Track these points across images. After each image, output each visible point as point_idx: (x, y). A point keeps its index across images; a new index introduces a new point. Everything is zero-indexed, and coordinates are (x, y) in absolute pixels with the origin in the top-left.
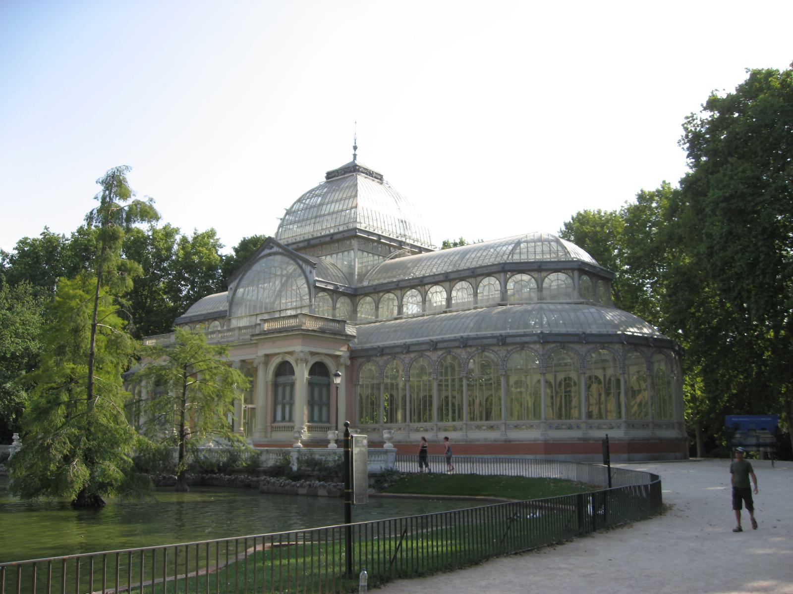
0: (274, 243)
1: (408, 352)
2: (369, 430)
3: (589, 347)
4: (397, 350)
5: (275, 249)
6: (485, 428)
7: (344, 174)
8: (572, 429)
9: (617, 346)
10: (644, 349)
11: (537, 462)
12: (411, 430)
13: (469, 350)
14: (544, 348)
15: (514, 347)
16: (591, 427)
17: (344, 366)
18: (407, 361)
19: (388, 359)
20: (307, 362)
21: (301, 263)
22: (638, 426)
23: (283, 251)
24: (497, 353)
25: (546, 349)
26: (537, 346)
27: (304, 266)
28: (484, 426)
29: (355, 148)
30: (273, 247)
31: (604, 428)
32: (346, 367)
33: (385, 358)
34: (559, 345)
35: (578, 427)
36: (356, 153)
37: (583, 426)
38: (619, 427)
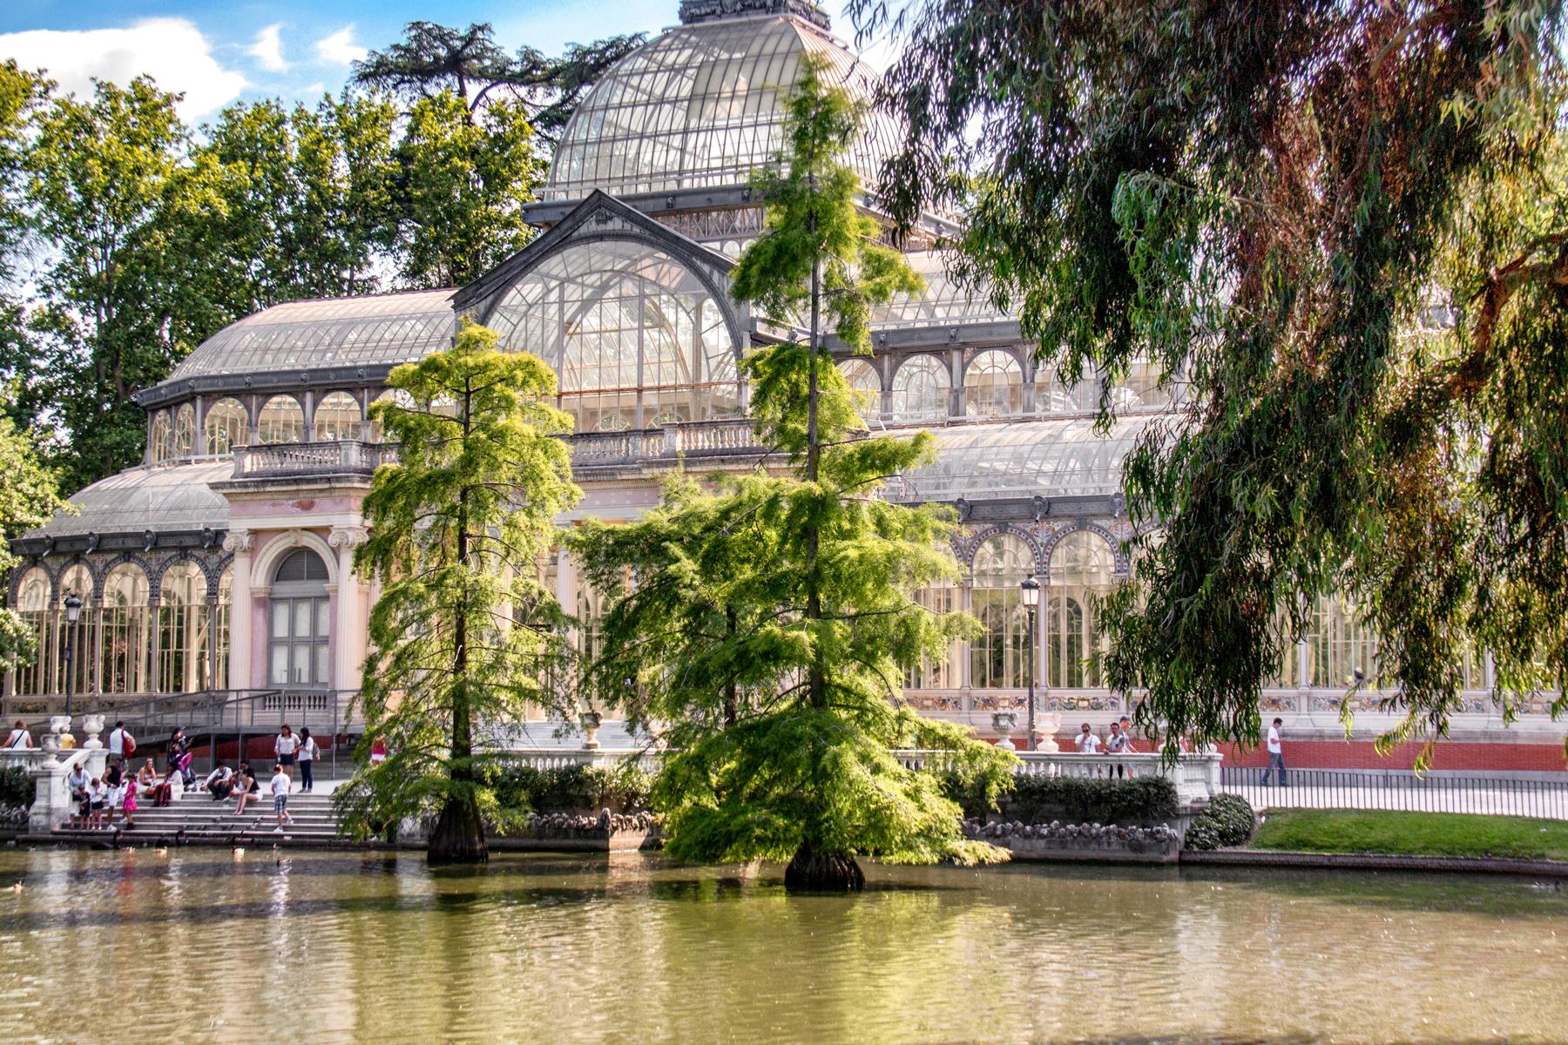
0: (612, 210)
1: (1047, 515)
2: (929, 703)
4: (1014, 511)
5: (616, 224)
7: (739, 13)
11: (1387, 784)
12: (1053, 705)
18: (1041, 538)
19: (985, 531)
21: (706, 268)
23: (647, 234)
27: (716, 276)
30: (611, 218)
33: (977, 528)
35: (1479, 708)
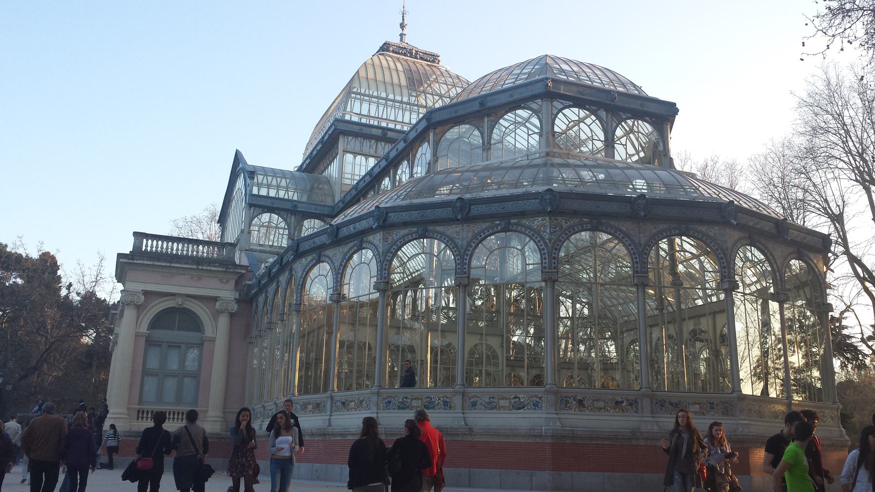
3: (477, 227)
6: (310, 407)
8: (433, 408)
9: (537, 222)
10: (625, 226)
13: (304, 261)
14: (385, 239)
15: (352, 244)
16: (474, 404)
17: (225, 315)
20: (139, 308)
22: (601, 404)
24: (332, 262)
25: (390, 241)
26: (377, 238)
28: (310, 404)
29: (402, 26)
31: (504, 408)
32: (232, 315)
34: (415, 229)
36: (404, 33)
37: (457, 401)
38: (536, 405)
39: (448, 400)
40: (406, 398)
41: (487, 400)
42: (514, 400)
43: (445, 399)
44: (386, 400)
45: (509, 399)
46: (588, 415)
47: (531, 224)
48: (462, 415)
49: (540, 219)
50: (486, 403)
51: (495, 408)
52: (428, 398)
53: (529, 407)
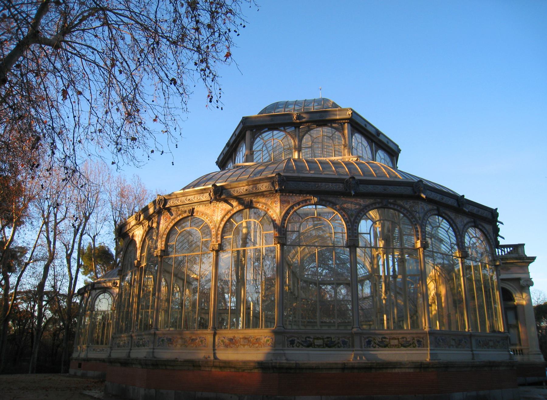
3: (362, 202)
39: (346, 340)
40: (309, 337)
41: (380, 340)
42: (403, 340)
43: (343, 339)
44: (291, 339)
45: (398, 339)
46: (448, 350)
47: (405, 204)
48: (471, 353)
49: (411, 201)
50: (379, 342)
51: (386, 346)
52: (328, 338)
53: (414, 346)
